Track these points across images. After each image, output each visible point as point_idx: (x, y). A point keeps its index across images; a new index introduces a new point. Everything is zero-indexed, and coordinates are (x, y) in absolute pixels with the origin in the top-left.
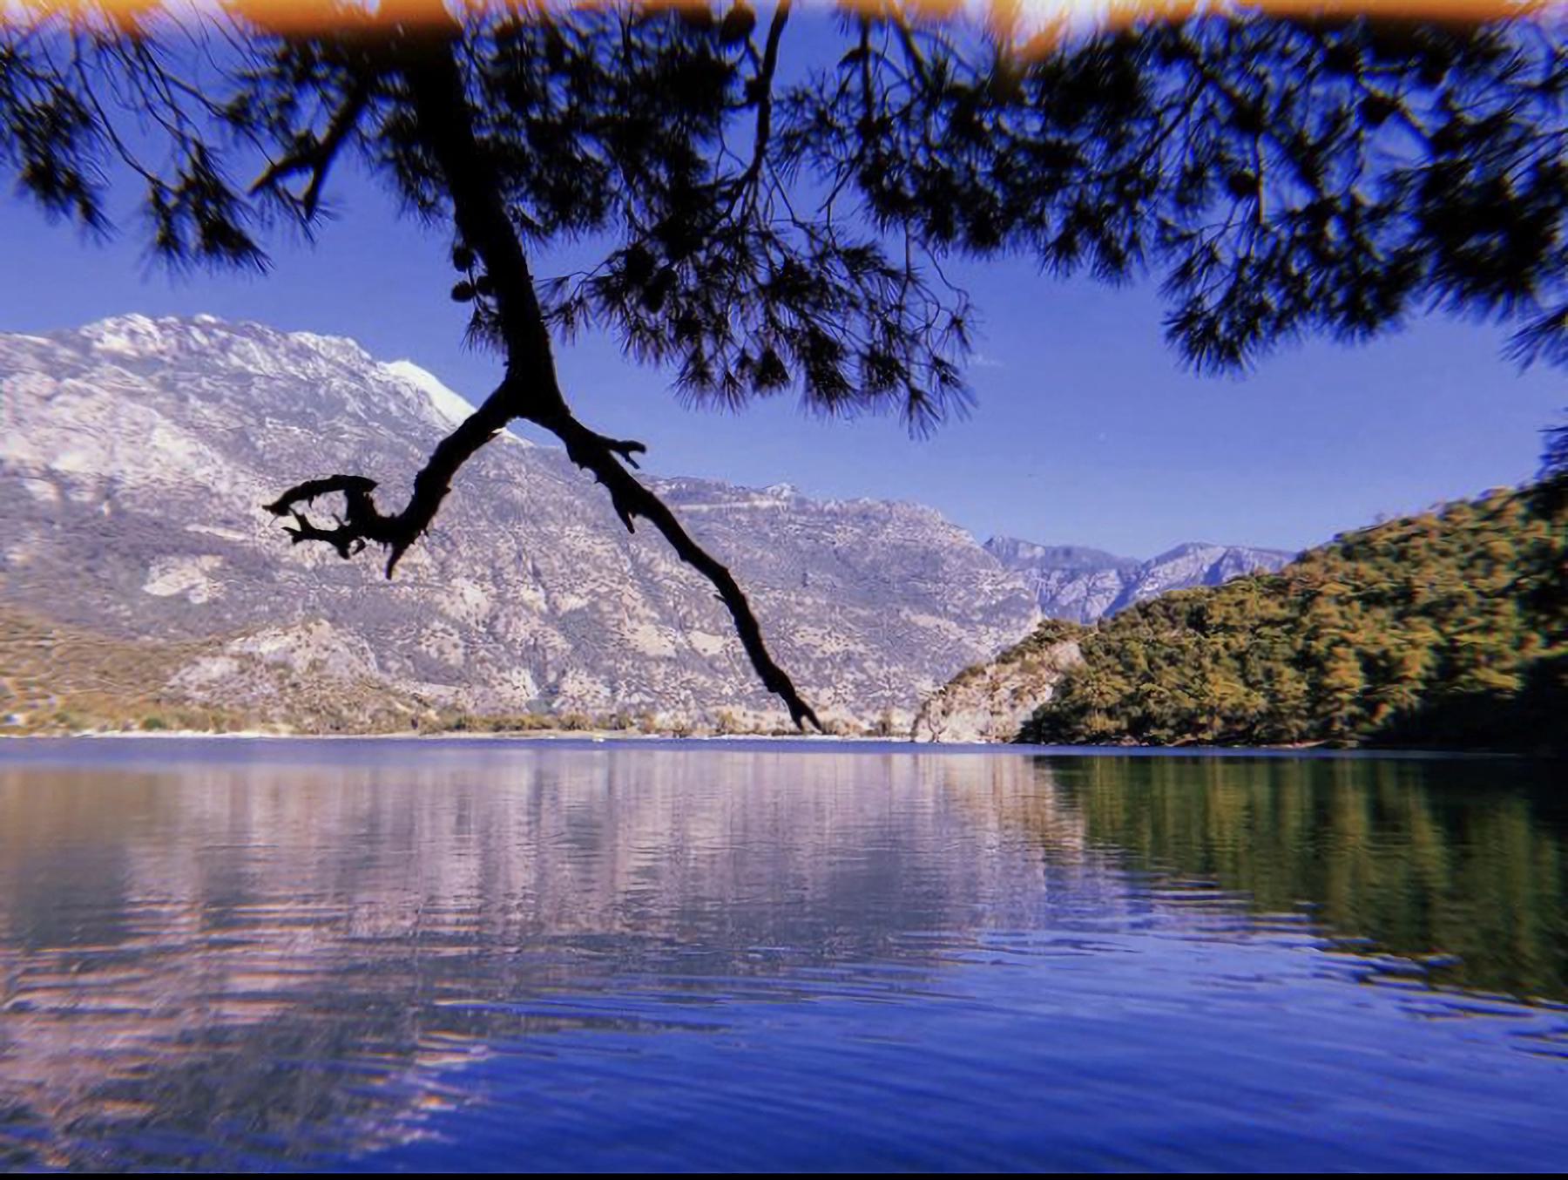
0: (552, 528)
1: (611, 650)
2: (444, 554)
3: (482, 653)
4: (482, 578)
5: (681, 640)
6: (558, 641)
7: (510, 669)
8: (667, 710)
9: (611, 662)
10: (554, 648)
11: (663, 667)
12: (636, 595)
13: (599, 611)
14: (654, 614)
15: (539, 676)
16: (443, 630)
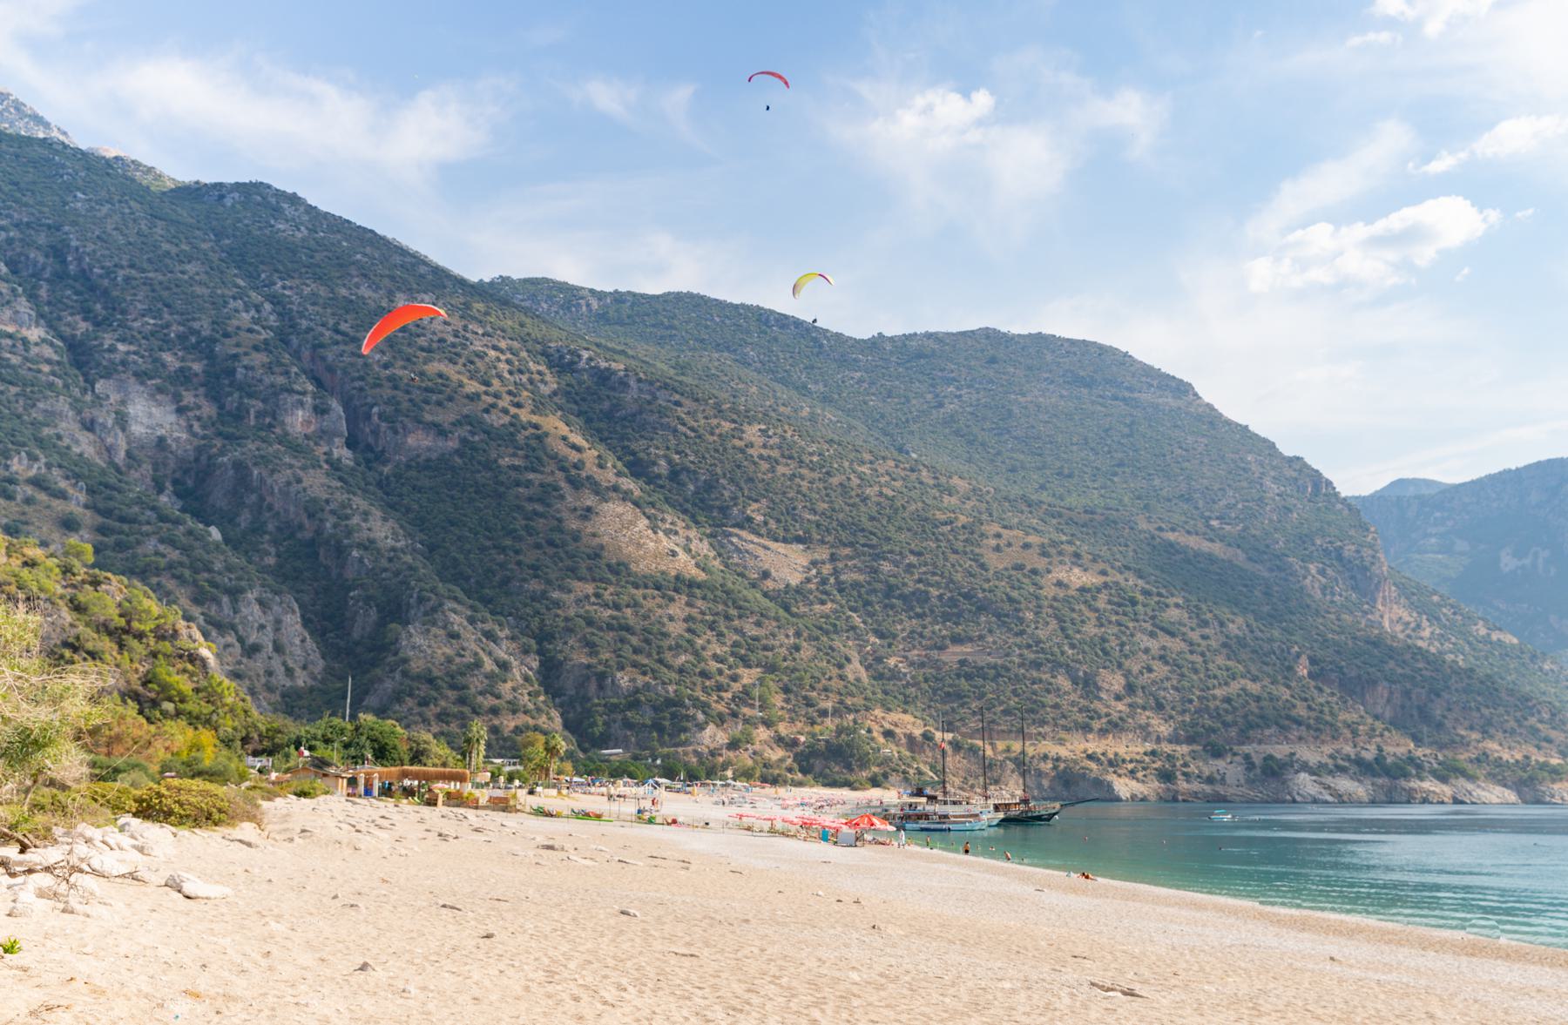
0: (365, 291)
1: (530, 557)
2: (83, 326)
3: (151, 545)
4: (183, 377)
5: (704, 548)
6: (381, 530)
7: (235, 593)
8: (720, 720)
9: (534, 586)
10: (368, 546)
11: (678, 609)
12: (577, 439)
13: (489, 465)
14: (627, 483)
15: (326, 622)
16: (37, 482)
